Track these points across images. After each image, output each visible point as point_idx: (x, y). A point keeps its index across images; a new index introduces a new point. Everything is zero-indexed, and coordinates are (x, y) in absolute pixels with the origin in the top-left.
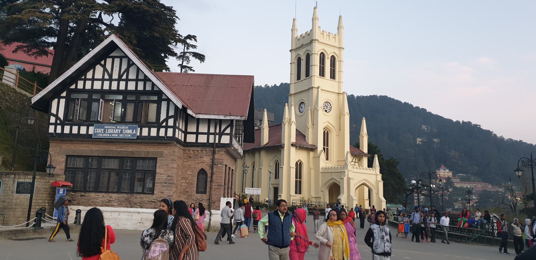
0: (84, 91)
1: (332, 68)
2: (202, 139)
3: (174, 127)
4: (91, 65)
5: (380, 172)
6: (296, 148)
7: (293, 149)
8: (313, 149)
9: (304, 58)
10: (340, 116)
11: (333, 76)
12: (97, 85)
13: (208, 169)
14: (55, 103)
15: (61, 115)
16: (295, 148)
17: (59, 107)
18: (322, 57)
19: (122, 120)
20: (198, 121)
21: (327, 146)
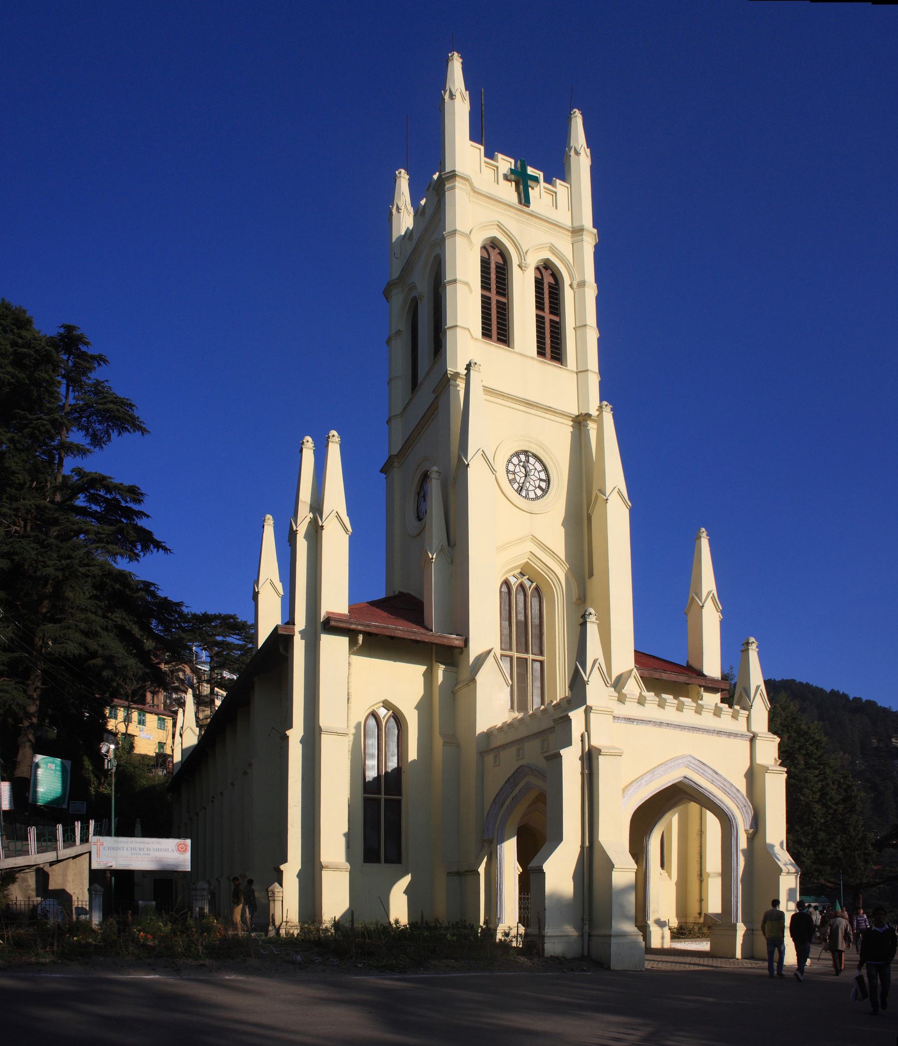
5: (773, 728)
6: (353, 643)
7: (334, 647)
11: (551, 345)
16: (344, 641)
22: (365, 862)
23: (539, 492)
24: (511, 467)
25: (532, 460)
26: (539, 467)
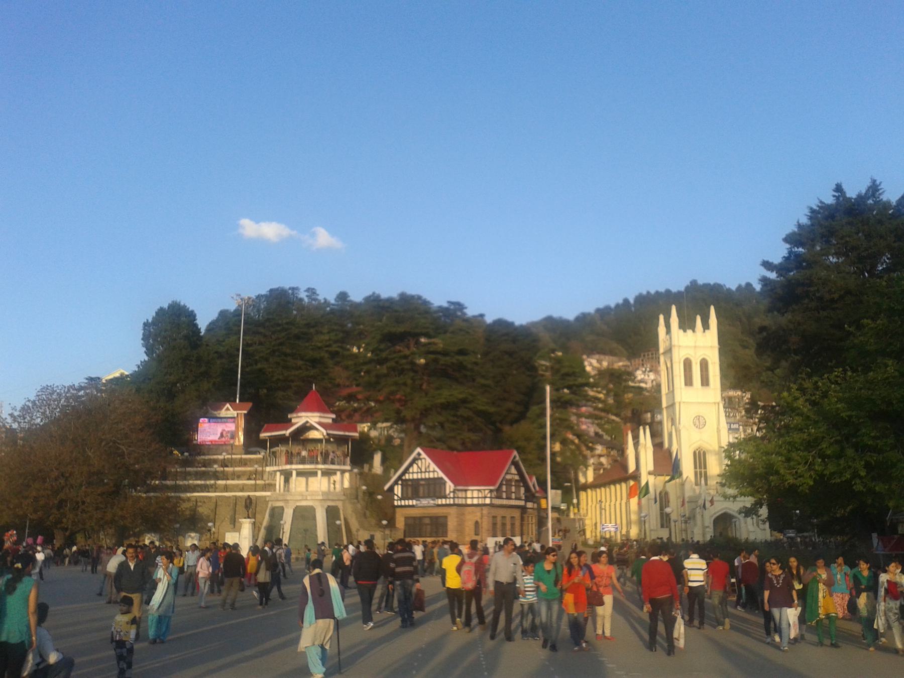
0: (409, 480)
2: (475, 501)
3: (454, 498)
4: (411, 465)
9: (669, 365)
10: (718, 431)
12: (415, 476)
13: (479, 521)
14: (396, 487)
15: (400, 495)
17: (398, 490)
18: (688, 364)
19: (429, 497)
20: (472, 490)
21: (705, 467)
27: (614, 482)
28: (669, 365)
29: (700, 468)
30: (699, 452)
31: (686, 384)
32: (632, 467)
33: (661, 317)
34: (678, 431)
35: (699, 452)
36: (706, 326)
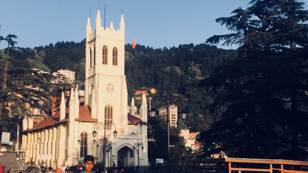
1: (115, 57)
8: (95, 121)
9: (93, 50)
21: (112, 118)
22: (81, 157)
23: (112, 91)
24: (107, 87)
25: (111, 85)
26: (112, 86)
27: (48, 128)
28: (93, 50)
29: (108, 118)
30: (109, 108)
31: (103, 63)
32: (63, 117)
33: (89, 19)
34: (97, 93)
35: (109, 108)
36: (117, 27)
